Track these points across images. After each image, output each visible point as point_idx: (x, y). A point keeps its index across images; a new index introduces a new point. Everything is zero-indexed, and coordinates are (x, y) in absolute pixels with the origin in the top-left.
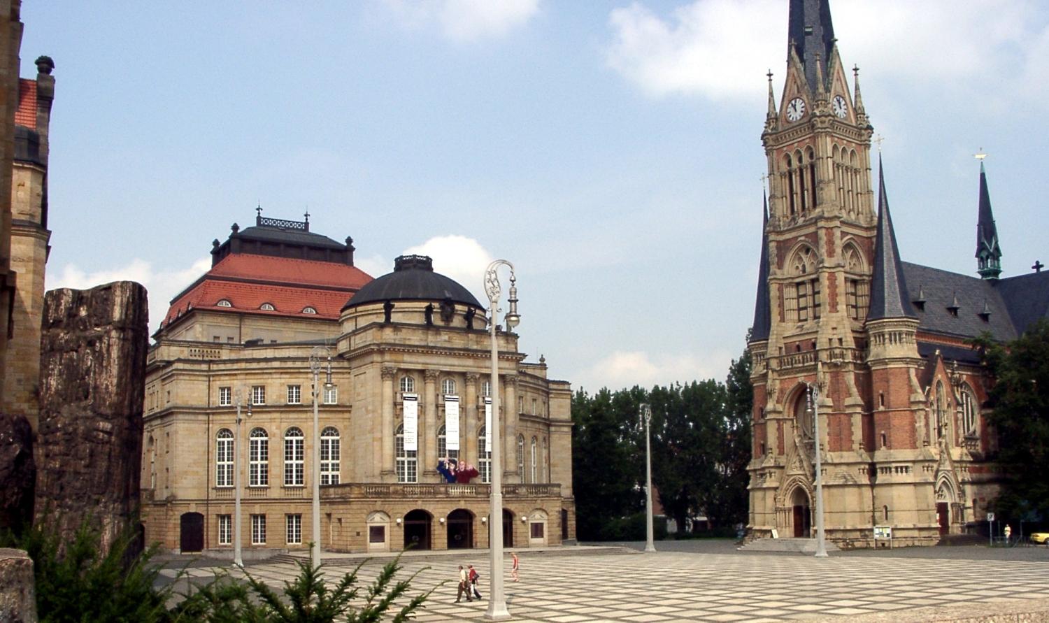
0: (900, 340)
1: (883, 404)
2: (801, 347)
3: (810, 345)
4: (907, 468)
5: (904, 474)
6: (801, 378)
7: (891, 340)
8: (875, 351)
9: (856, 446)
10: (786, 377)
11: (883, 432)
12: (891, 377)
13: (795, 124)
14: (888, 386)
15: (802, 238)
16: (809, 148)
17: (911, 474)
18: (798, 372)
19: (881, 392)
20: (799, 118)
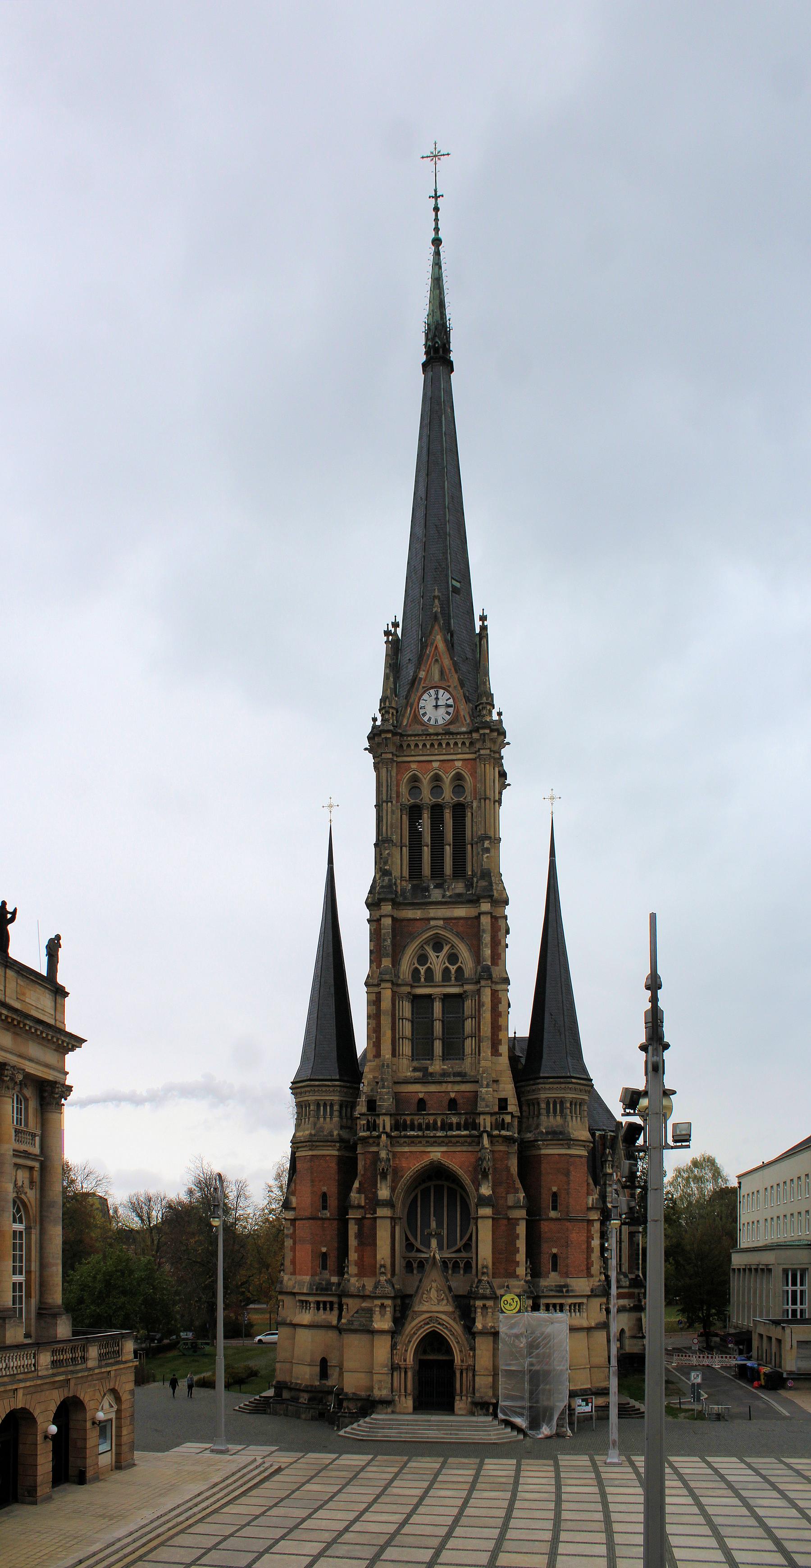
0: (562, 1111)
1: (555, 1208)
2: (429, 1103)
3: (445, 1103)
4: (580, 1304)
5: (578, 1314)
6: (436, 1153)
7: (548, 1112)
8: (548, 1122)
9: (521, 1271)
10: (406, 1149)
11: (555, 1251)
12: (571, 1168)
13: (431, 731)
14: (568, 1183)
15: (441, 923)
16: (459, 777)
17: (585, 1315)
18: (432, 1145)
19: (555, 1189)
20: (441, 722)
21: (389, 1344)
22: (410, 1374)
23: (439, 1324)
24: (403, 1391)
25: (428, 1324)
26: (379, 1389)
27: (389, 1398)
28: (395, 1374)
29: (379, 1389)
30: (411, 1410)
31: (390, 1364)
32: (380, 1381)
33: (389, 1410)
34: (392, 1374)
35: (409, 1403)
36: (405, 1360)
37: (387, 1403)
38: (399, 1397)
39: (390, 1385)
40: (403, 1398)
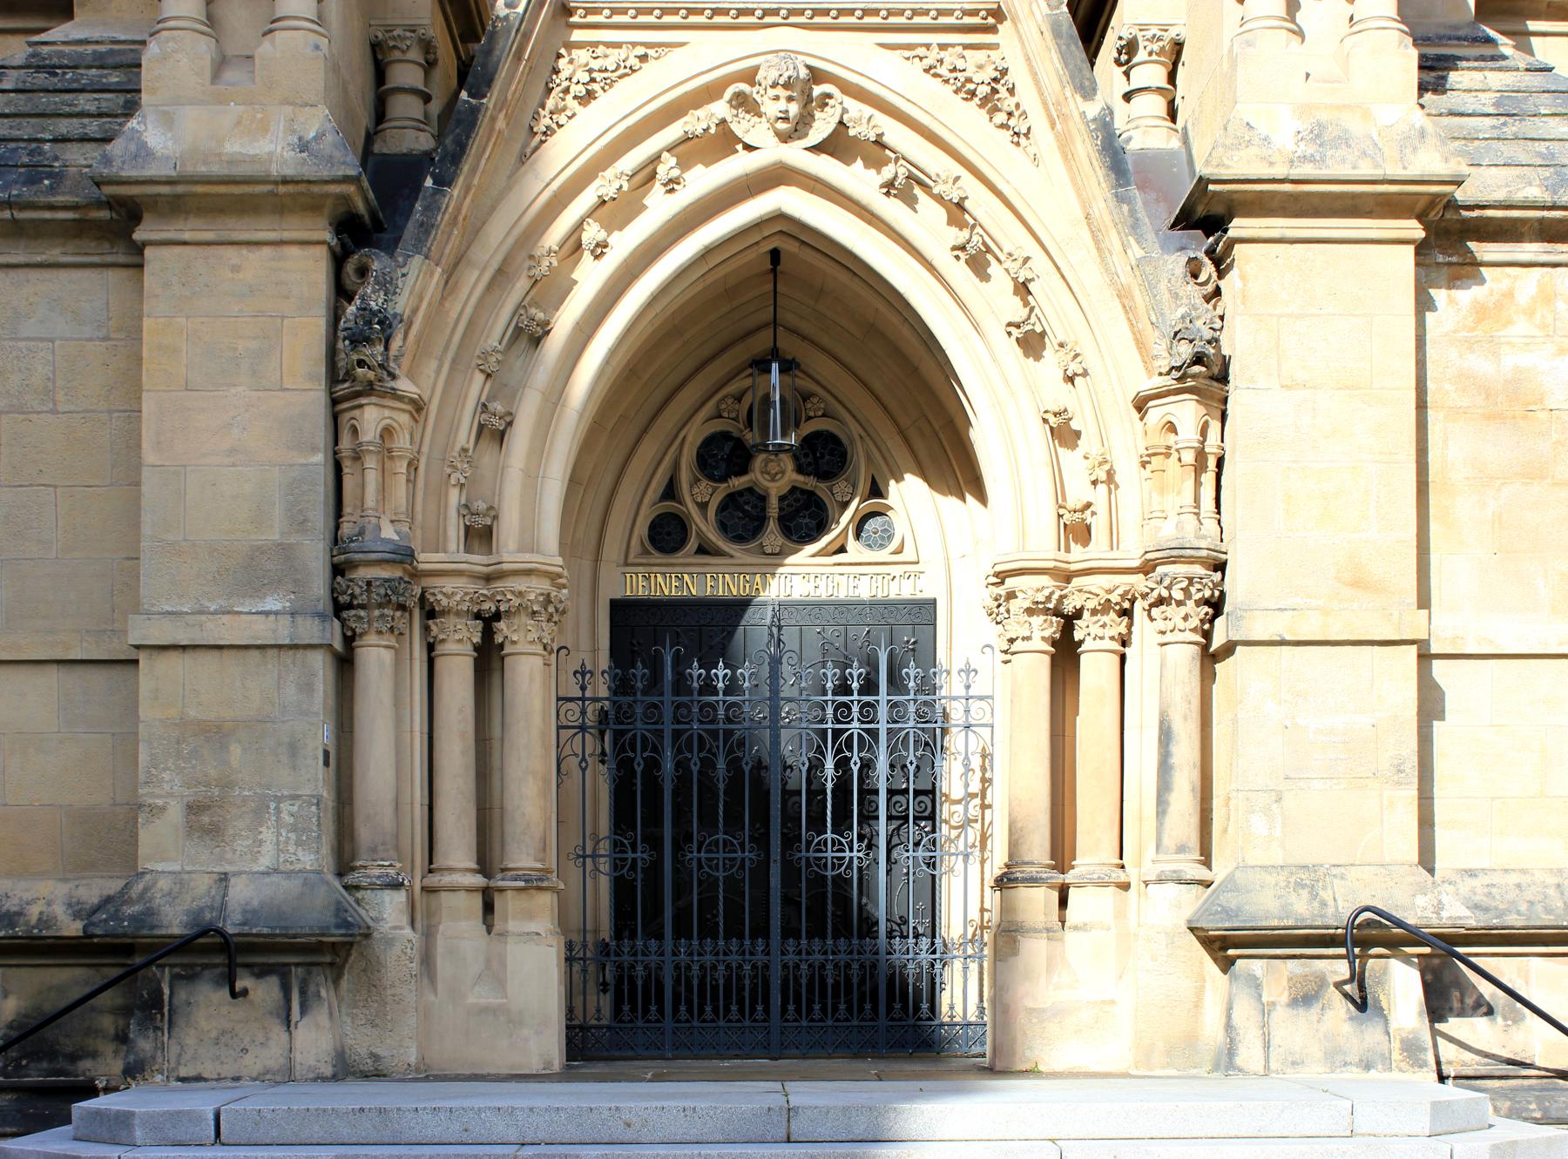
21: (306, 336)
22: (530, 682)
23: (838, 145)
24: (458, 849)
25: (725, 141)
26: (204, 819)
27: (313, 912)
28: (375, 657)
29: (204, 819)
30: (545, 1043)
31: (315, 556)
32: (216, 734)
33: (314, 1039)
34: (345, 663)
35: (526, 972)
36: (480, 535)
37: (305, 957)
38: (422, 916)
39: (316, 780)
40: (459, 921)
